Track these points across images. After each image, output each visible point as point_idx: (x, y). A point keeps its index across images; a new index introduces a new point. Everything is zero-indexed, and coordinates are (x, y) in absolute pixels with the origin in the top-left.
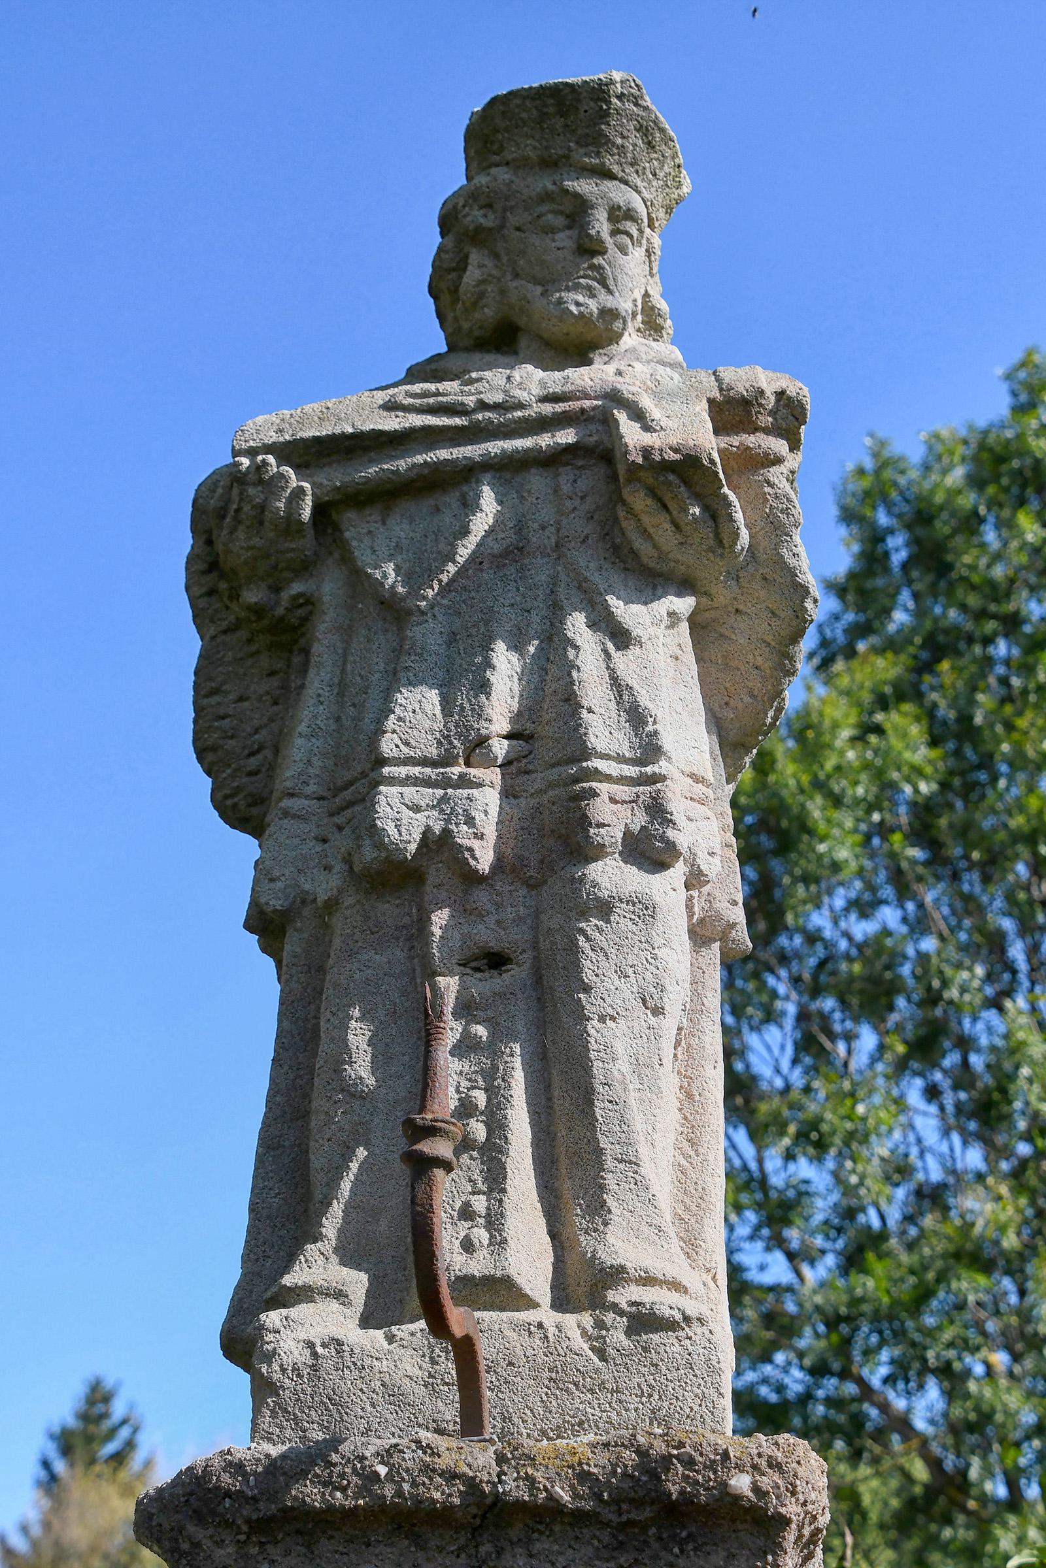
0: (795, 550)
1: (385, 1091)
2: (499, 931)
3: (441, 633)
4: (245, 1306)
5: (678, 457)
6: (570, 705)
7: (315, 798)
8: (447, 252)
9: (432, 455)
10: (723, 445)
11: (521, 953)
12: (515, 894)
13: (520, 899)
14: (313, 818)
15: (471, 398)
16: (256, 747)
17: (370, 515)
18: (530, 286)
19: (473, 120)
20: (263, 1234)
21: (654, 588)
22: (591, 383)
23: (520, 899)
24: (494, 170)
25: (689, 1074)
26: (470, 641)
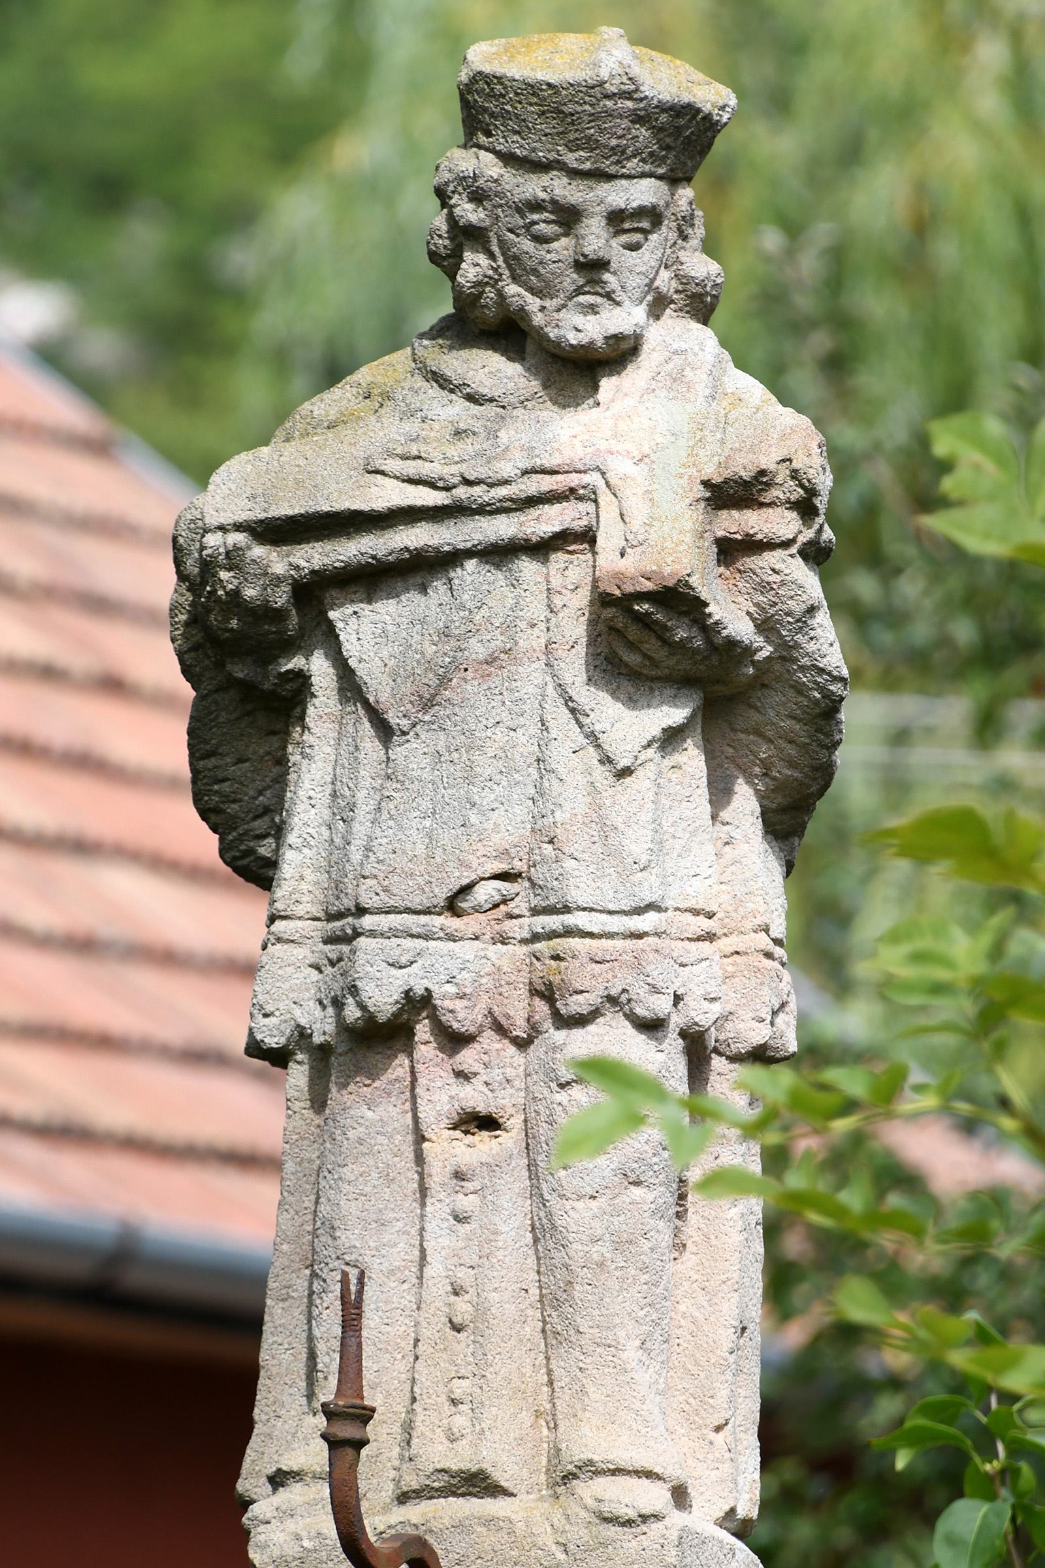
0: (812, 634)
1: (379, 1261)
2: (489, 1093)
3: (425, 754)
4: (257, 1468)
7: (308, 919)
12: (502, 1053)
13: (506, 1060)
14: (308, 941)
16: (261, 810)
17: (355, 593)
20: (273, 1393)
21: (652, 690)
23: (506, 1060)
25: (706, 1214)
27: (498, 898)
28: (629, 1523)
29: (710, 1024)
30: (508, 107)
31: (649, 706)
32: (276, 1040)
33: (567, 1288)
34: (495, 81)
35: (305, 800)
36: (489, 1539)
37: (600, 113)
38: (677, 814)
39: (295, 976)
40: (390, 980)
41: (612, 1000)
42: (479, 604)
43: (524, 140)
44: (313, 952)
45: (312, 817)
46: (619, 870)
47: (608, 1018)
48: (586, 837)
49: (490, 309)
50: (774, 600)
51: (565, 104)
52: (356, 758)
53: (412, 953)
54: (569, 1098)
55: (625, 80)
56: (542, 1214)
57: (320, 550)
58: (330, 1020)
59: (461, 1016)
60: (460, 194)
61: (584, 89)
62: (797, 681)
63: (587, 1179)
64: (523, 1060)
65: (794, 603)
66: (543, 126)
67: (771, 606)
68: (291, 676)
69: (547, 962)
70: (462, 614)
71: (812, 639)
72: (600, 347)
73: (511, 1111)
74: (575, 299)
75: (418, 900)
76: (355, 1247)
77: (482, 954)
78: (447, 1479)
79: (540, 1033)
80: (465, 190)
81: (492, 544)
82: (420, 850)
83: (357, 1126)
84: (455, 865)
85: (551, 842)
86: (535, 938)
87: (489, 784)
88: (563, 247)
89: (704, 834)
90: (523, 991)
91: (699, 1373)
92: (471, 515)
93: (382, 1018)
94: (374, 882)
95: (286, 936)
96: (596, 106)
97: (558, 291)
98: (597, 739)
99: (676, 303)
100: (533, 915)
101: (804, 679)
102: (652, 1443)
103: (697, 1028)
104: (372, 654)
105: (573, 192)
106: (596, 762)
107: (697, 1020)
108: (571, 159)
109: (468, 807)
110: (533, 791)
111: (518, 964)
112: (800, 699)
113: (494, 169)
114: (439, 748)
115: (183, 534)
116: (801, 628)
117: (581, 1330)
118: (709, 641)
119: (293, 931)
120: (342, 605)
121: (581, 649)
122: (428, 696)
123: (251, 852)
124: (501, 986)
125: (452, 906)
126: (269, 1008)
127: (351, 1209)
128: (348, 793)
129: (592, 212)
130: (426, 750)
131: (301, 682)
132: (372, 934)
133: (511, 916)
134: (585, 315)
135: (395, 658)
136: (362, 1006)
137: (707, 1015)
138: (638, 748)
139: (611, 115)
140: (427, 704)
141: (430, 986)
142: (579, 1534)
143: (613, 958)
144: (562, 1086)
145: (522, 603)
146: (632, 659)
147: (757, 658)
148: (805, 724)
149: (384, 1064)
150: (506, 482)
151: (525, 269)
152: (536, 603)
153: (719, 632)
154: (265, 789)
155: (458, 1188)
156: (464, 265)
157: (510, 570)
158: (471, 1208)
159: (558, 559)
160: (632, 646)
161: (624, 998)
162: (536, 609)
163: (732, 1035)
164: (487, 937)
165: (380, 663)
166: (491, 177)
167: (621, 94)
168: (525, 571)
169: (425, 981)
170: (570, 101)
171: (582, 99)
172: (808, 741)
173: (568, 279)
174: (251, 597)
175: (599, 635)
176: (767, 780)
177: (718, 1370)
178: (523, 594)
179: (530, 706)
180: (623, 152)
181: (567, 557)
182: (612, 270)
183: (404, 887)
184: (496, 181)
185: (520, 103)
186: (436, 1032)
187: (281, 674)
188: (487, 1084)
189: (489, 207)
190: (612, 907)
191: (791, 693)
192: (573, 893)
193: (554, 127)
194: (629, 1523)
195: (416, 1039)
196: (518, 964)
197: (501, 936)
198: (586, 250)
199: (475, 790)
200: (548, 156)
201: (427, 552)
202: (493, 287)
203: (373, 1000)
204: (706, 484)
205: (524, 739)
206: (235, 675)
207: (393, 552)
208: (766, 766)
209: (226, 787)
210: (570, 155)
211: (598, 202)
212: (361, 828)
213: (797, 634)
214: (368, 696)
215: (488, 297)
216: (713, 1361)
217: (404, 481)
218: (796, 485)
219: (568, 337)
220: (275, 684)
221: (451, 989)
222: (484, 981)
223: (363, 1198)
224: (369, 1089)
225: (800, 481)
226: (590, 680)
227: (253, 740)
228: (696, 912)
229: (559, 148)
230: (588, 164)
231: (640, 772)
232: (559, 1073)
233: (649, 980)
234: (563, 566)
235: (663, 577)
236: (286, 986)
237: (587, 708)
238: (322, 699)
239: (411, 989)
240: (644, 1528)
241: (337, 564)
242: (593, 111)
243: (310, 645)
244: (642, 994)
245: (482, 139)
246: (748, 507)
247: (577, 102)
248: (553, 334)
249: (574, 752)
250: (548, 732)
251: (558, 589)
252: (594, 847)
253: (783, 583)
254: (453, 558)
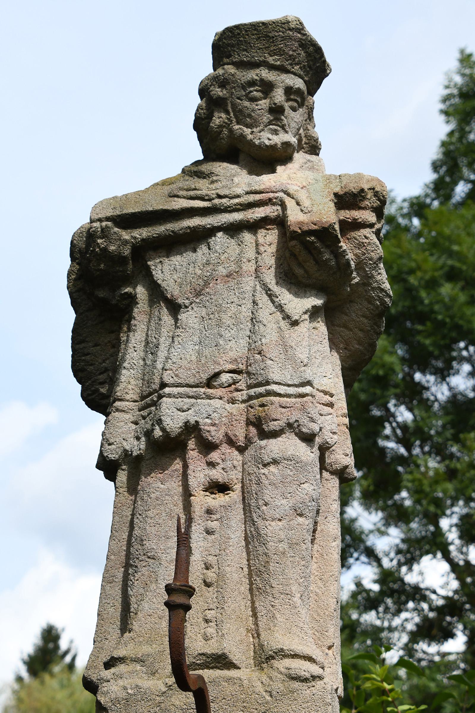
0: (379, 271)
1: (165, 556)
3: (196, 317)
4: (95, 664)
5: (316, 227)
6: (261, 356)
7: (132, 401)
8: (202, 109)
9: (192, 222)
10: (342, 218)
11: (234, 485)
14: (131, 411)
15: (213, 192)
16: (103, 369)
18: (245, 129)
19: (216, 38)
20: (104, 627)
21: (305, 292)
22: (275, 184)
23: (234, 457)
24: (226, 67)
25: (321, 544)
26: (210, 322)
27: (231, 381)
28: (306, 680)
29: (333, 444)
30: (242, 39)
31: (305, 297)
32: (114, 456)
33: (266, 565)
34: (235, 29)
35: (132, 348)
36: (229, 689)
37: (287, 36)
38: (316, 348)
39: (124, 427)
40: (178, 417)
41: (290, 425)
42: (223, 252)
43: (248, 53)
44: (133, 416)
45: (135, 356)
46: (293, 365)
47: (287, 435)
48: (277, 351)
49: (224, 140)
50: (364, 251)
51: (270, 32)
52: (159, 325)
53: (189, 405)
54: (269, 471)
55: (298, 23)
56: (252, 529)
57: (146, 230)
58: (143, 443)
59: (213, 434)
60: (214, 85)
61: (280, 25)
62: (369, 296)
63: (277, 510)
64: (241, 458)
65: (374, 254)
66: (258, 45)
67: (363, 255)
68: (126, 296)
69: (257, 408)
70: (215, 254)
71: (379, 274)
72: (279, 148)
73: (236, 481)
74: (268, 127)
75: (192, 380)
76: (153, 549)
77: (224, 406)
78: (205, 659)
79: (252, 443)
80: (216, 83)
81: (231, 223)
82: (194, 358)
83: (155, 492)
84: (212, 363)
85: (260, 353)
86: (250, 398)
87: (228, 328)
88: (264, 104)
89: (328, 360)
90: (243, 424)
91: (320, 619)
92: (220, 213)
93: (173, 435)
94: (171, 372)
95: (121, 408)
96: (285, 33)
97: (260, 123)
98: (282, 307)
99: (304, 149)
100: (248, 389)
101: (373, 295)
102: (309, 644)
103: (327, 445)
104: (169, 278)
105: (270, 76)
106: (281, 319)
107: (328, 440)
108: (271, 60)
109: (219, 337)
110: (249, 333)
111: (241, 411)
112: (370, 306)
113: (232, 70)
114: (203, 315)
115: (76, 239)
116: (375, 267)
117: (273, 586)
118: (337, 263)
119: (124, 406)
120: (154, 259)
121: (273, 269)
122: (199, 290)
123: (97, 390)
124: (232, 421)
125: (209, 383)
126: (111, 441)
127: (151, 530)
128: (155, 341)
129: (279, 86)
130: (196, 315)
131: (132, 299)
132: (169, 396)
133: (237, 390)
134: (272, 135)
135: (181, 278)
136: (163, 429)
137: (332, 439)
138: (301, 312)
139: (291, 39)
140: (198, 294)
141: (198, 419)
142: (278, 686)
143: (290, 406)
144: (265, 465)
145: (244, 250)
146: (299, 271)
147: (352, 282)
148: (369, 320)
149: (170, 463)
150: (238, 196)
151: (245, 116)
152: (250, 251)
153: (344, 256)
154: (106, 360)
155: (208, 518)
156: (214, 118)
157: (238, 238)
158: (215, 527)
159: (262, 232)
160: (300, 265)
161: (296, 425)
162: (251, 253)
163: (334, 461)
164: (226, 399)
165: (173, 281)
166: (231, 73)
167: (296, 29)
168: (246, 237)
169: (196, 417)
170: (273, 30)
171: (279, 29)
172: (369, 329)
173: (265, 118)
174: (113, 250)
175: (281, 265)
176: (346, 351)
177: (330, 618)
178: (245, 247)
179: (248, 296)
180: (294, 59)
181: (266, 231)
182: (285, 116)
183: (185, 375)
184: (233, 75)
185: (248, 35)
186: (199, 444)
187: (122, 294)
188: (223, 469)
189: (229, 88)
190: (290, 383)
191: (365, 303)
192: (271, 375)
193: (264, 45)
194: (306, 680)
195: (188, 448)
196: (241, 411)
197: (232, 399)
198: (276, 102)
199: (222, 329)
200: (260, 59)
201: (199, 228)
202: (227, 128)
203: (169, 425)
204: (336, 195)
205: (245, 310)
206: (99, 296)
207: (182, 229)
208: (347, 344)
209: (88, 358)
210: (271, 58)
211: (282, 81)
212: (162, 354)
213: (373, 270)
214: (167, 295)
215: (224, 133)
216: (327, 614)
217: (188, 199)
218: (377, 200)
219: (265, 142)
220: (118, 300)
221: (208, 421)
222: (223, 419)
223: (158, 526)
224: (162, 475)
225: (378, 197)
226: (278, 283)
227: (103, 336)
228: (325, 393)
229: (266, 55)
230: (279, 62)
231: (302, 325)
232: (264, 459)
233: (310, 415)
234: (264, 234)
235: (323, 223)
236: (120, 431)
237: (277, 294)
238: (141, 304)
239: (188, 422)
240: (313, 683)
241: (155, 235)
242: (283, 35)
243: (136, 282)
244: (306, 422)
245: (225, 60)
246: (353, 209)
247: (276, 31)
248: (257, 142)
249: (270, 314)
250: (257, 306)
251: (262, 244)
252: (281, 356)
253: (369, 244)
254: (212, 231)
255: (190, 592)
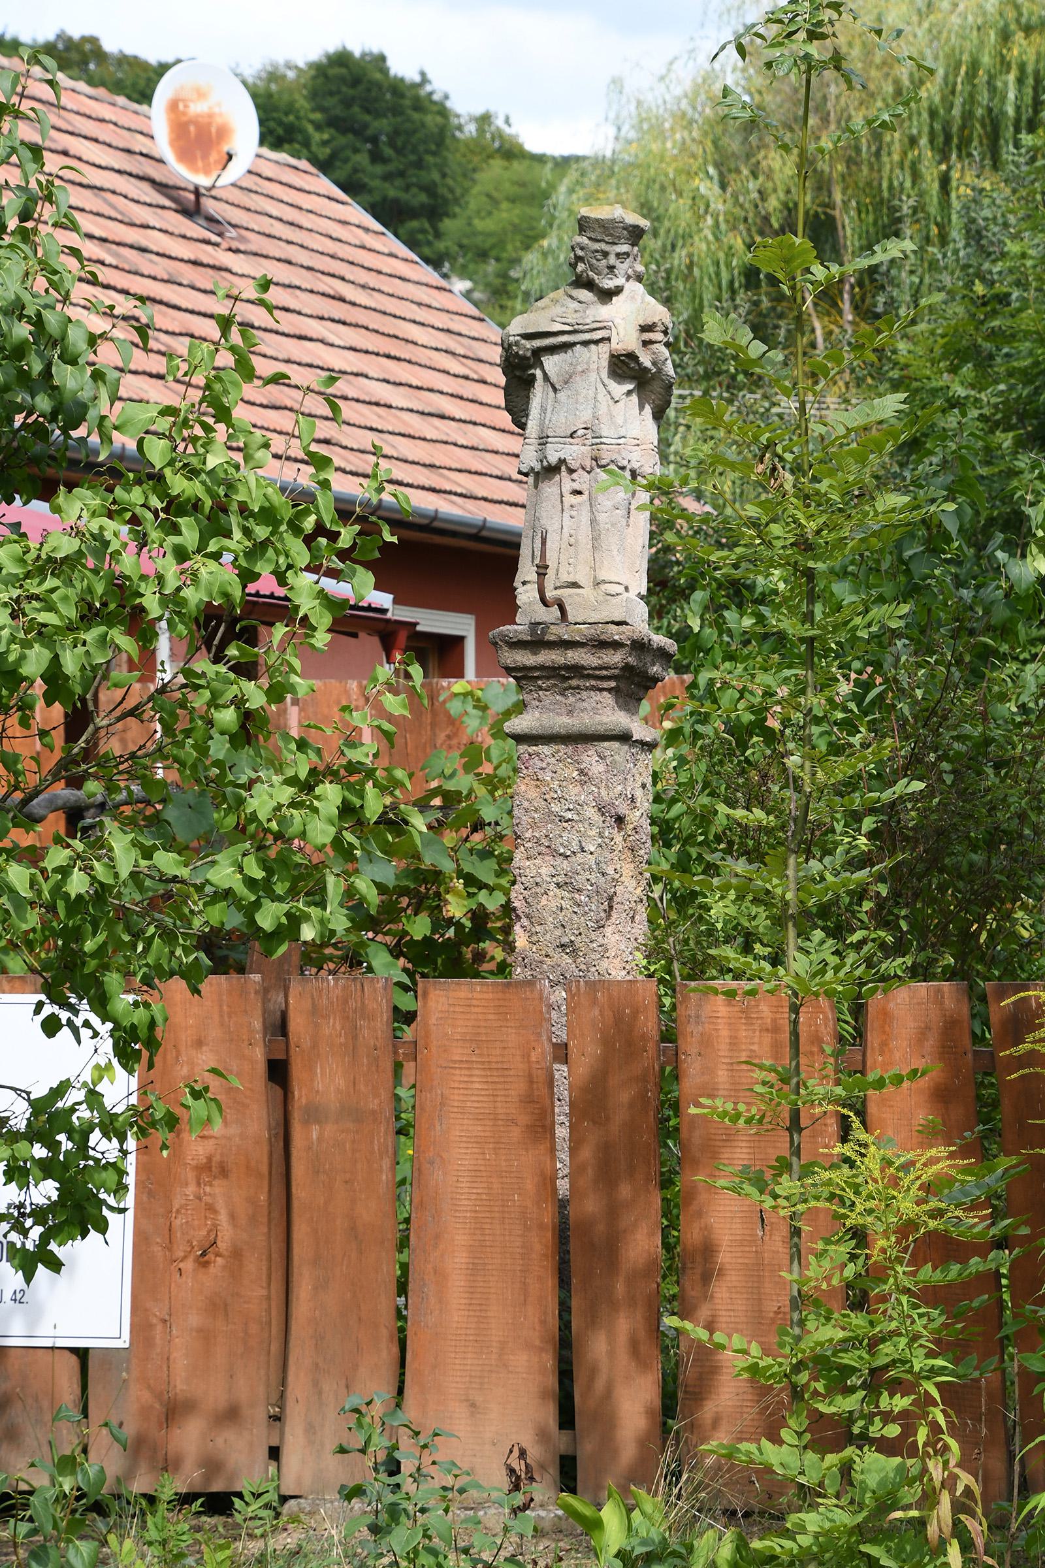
36: (577, 599)
88: (604, 262)
125: (571, 436)
127: (544, 514)
131: (534, 376)
142: (600, 598)
162: (595, 358)
212: (548, 415)
254: (574, 344)
255: (547, 567)
